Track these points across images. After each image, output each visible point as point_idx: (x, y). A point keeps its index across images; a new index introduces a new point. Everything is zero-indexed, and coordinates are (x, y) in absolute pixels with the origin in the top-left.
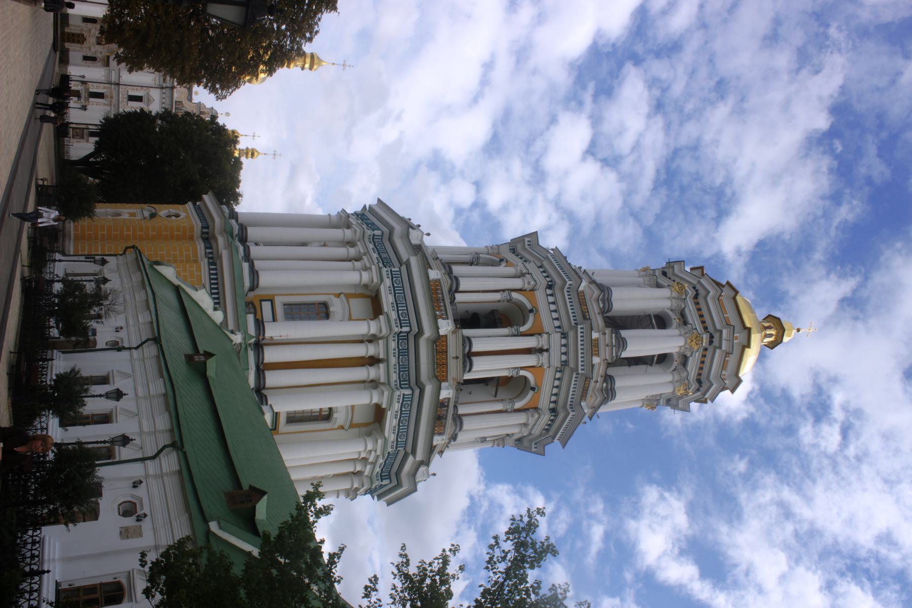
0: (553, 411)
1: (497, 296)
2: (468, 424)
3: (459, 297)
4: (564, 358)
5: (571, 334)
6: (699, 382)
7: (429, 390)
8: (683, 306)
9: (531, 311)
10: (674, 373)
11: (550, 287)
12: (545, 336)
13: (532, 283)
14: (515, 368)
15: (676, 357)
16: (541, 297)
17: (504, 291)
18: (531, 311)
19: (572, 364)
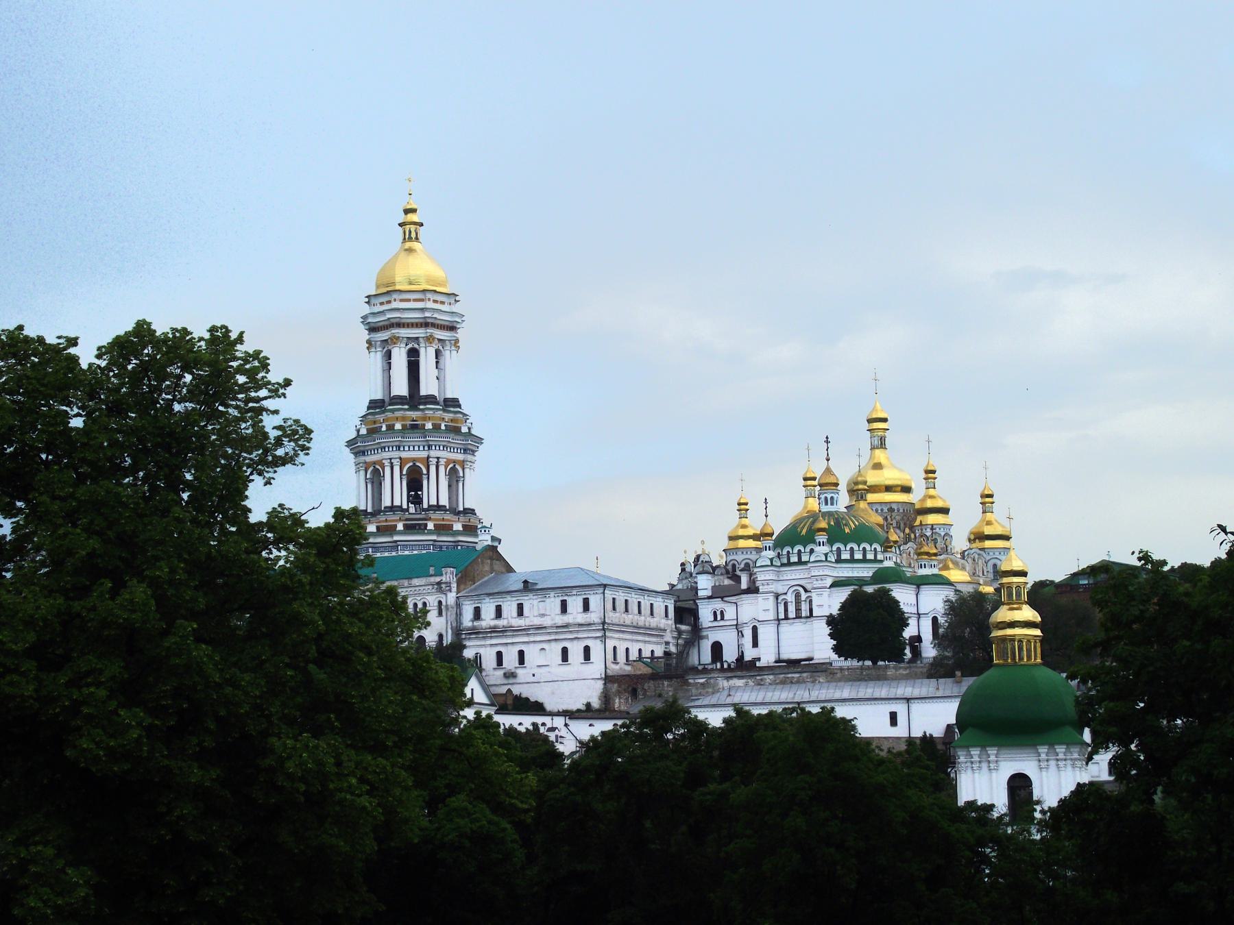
0: (430, 447)
1: (369, 486)
2: (433, 502)
3: (369, 510)
4: (394, 449)
5: (383, 445)
6: (425, 324)
7: (396, 538)
8: (379, 343)
9: (374, 467)
10: (421, 345)
11: (364, 452)
12: (384, 461)
13: (361, 465)
14: (401, 478)
15: (410, 346)
16: (369, 459)
17: (366, 482)
18: (374, 467)
19: (397, 443)
